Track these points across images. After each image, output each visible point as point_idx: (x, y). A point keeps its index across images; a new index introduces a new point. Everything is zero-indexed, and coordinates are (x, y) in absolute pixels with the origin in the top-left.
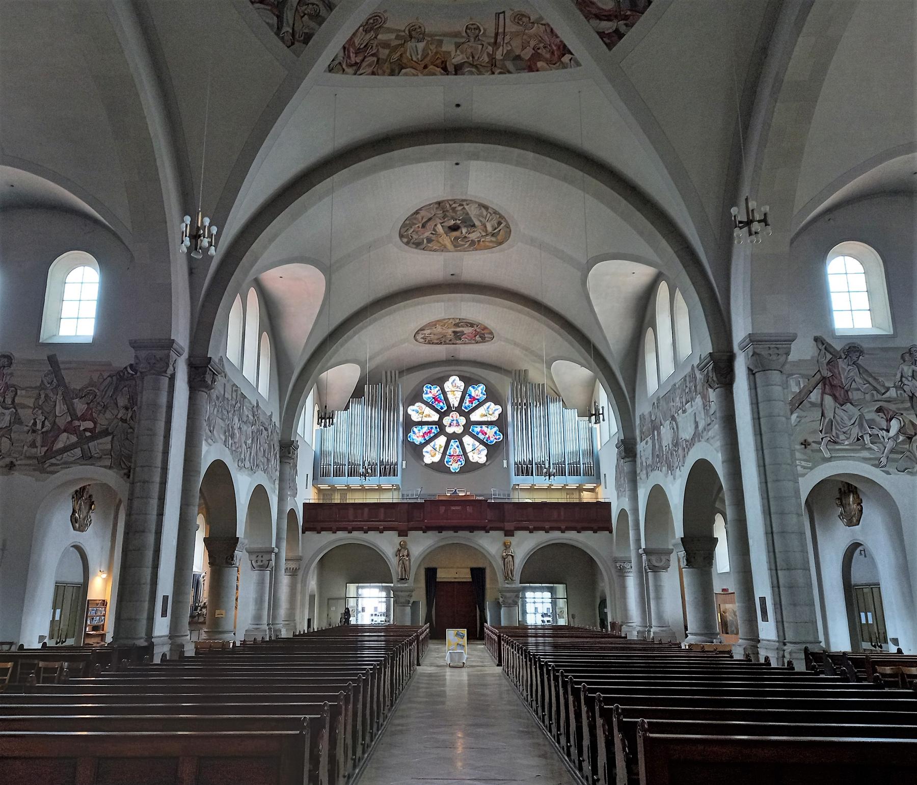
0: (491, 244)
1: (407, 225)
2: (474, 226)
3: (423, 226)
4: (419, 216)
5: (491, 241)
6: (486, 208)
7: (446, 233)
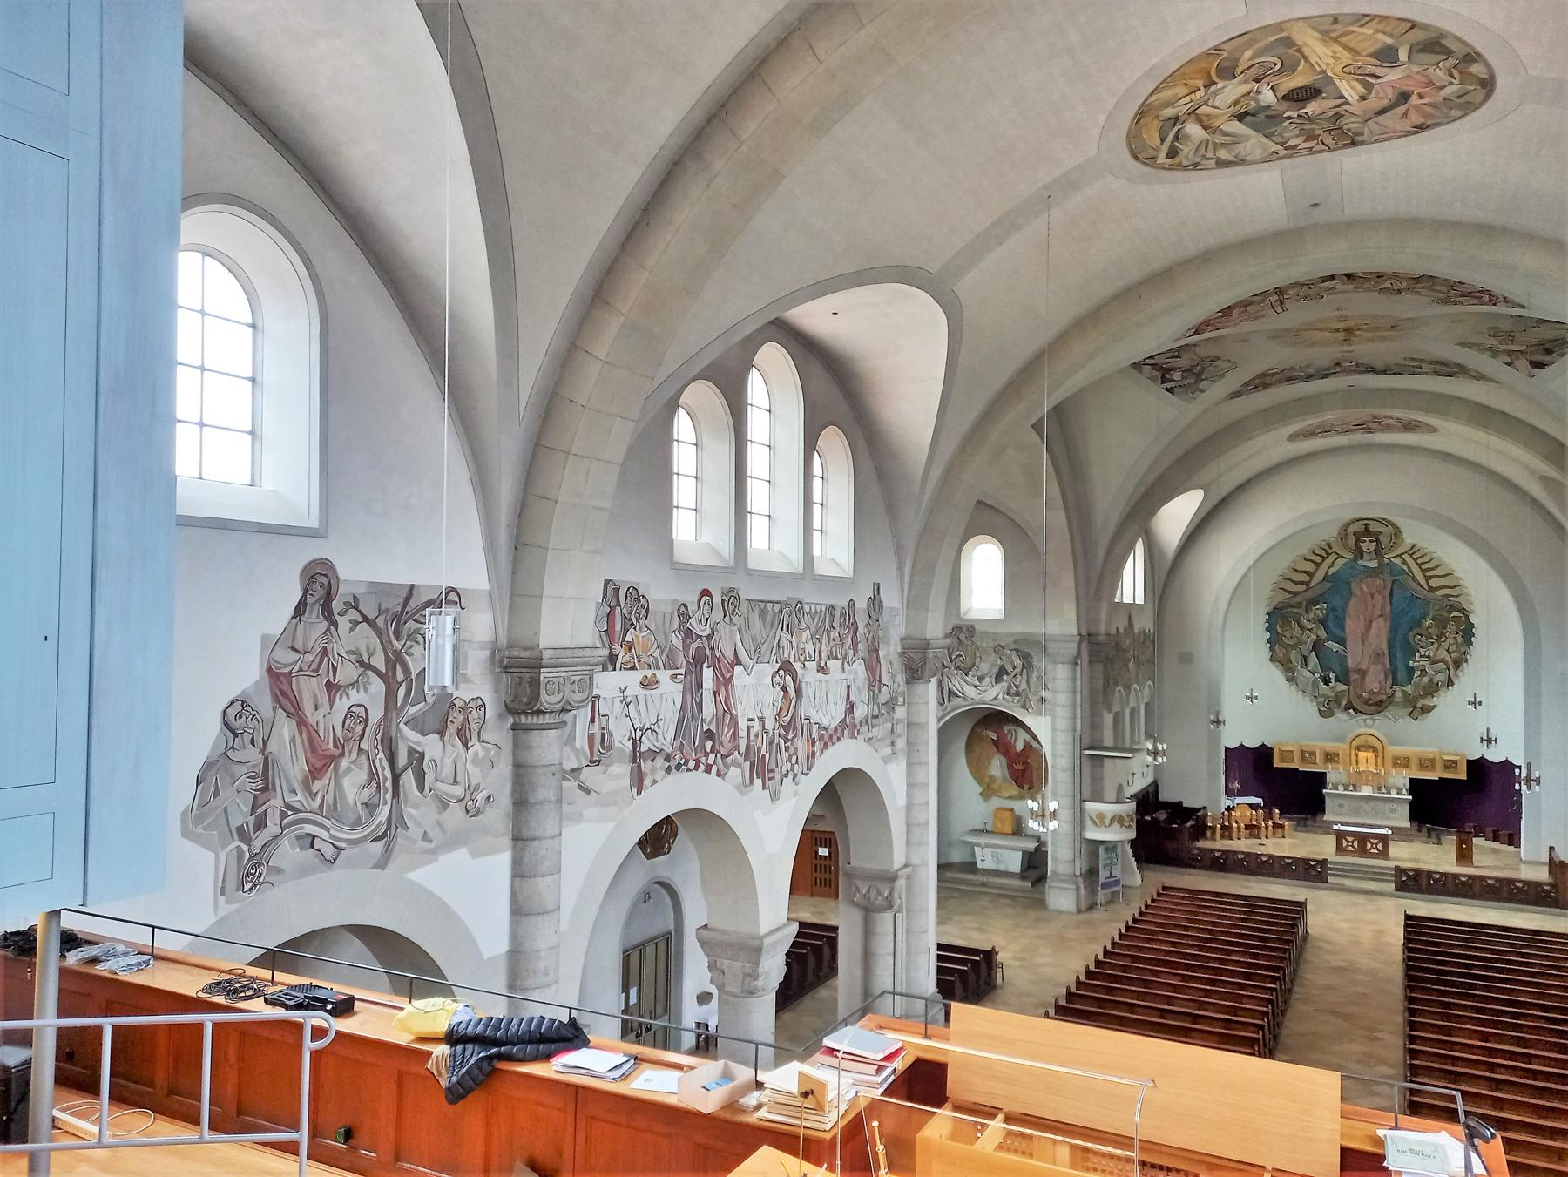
0: (1167, 94)
1: (1460, 107)
2: (1241, 117)
3: (1404, 97)
4: (1416, 118)
5: (1169, 104)
6: (1222, 164)
7: (1329, 80)
